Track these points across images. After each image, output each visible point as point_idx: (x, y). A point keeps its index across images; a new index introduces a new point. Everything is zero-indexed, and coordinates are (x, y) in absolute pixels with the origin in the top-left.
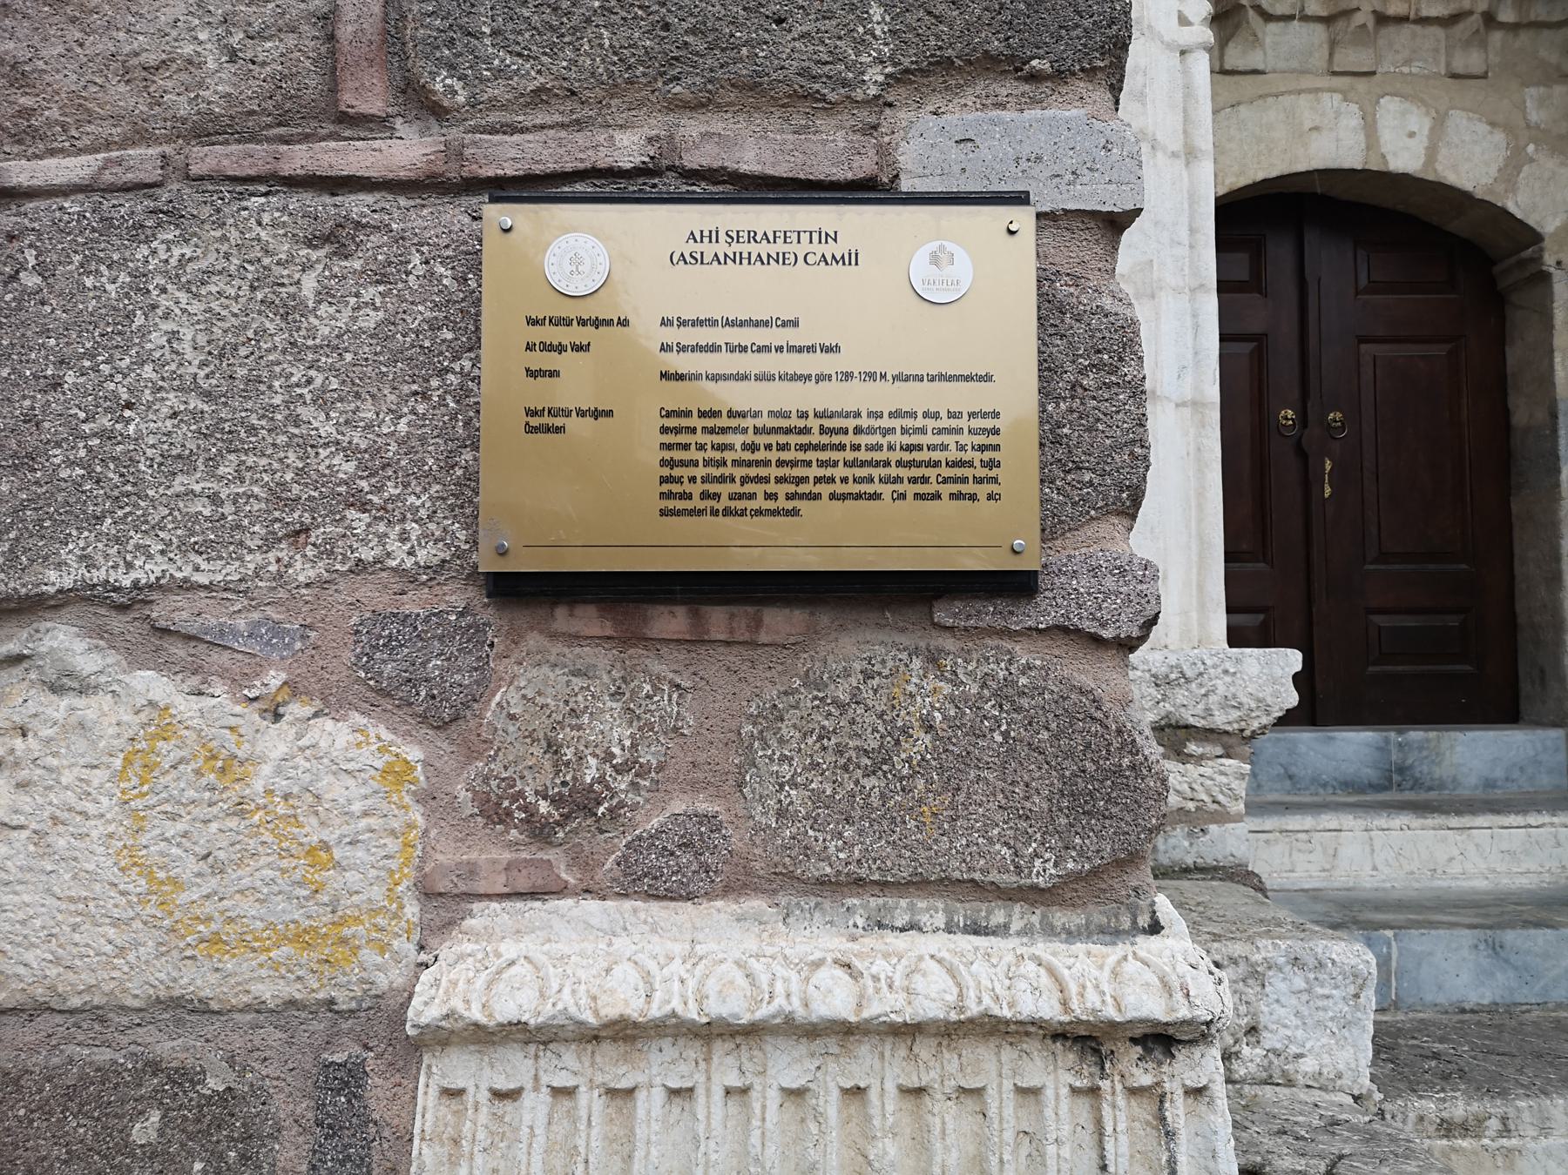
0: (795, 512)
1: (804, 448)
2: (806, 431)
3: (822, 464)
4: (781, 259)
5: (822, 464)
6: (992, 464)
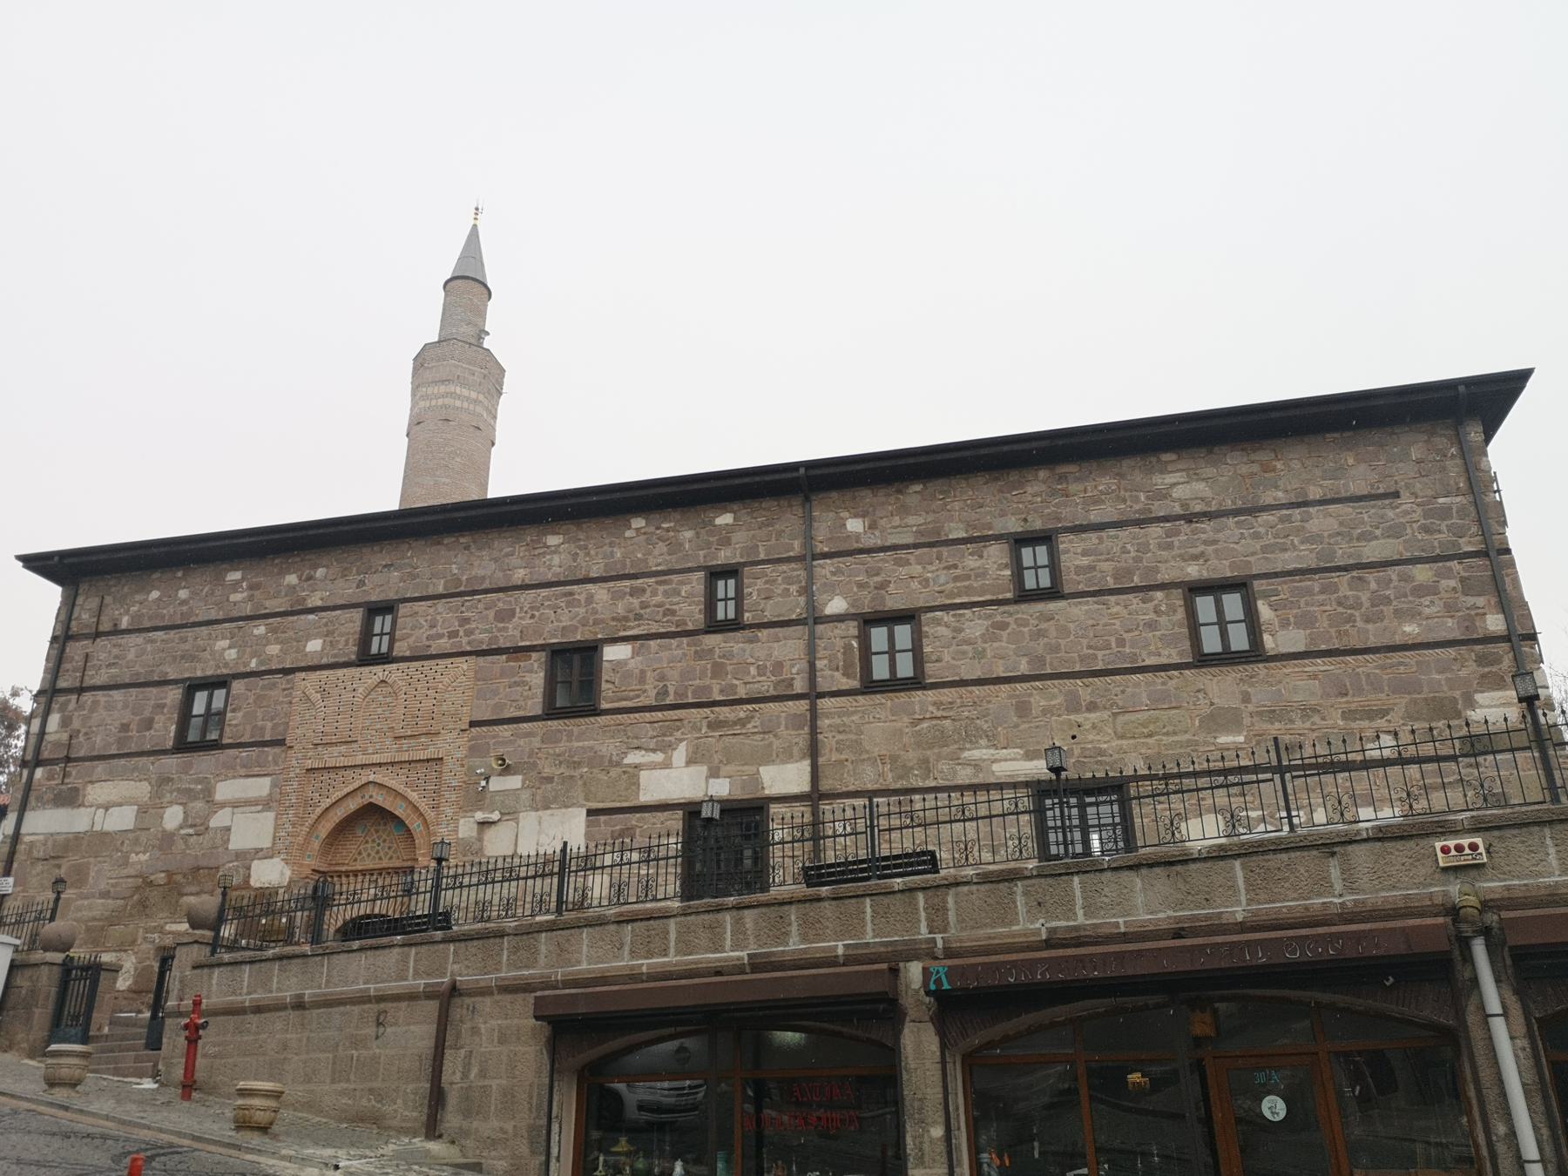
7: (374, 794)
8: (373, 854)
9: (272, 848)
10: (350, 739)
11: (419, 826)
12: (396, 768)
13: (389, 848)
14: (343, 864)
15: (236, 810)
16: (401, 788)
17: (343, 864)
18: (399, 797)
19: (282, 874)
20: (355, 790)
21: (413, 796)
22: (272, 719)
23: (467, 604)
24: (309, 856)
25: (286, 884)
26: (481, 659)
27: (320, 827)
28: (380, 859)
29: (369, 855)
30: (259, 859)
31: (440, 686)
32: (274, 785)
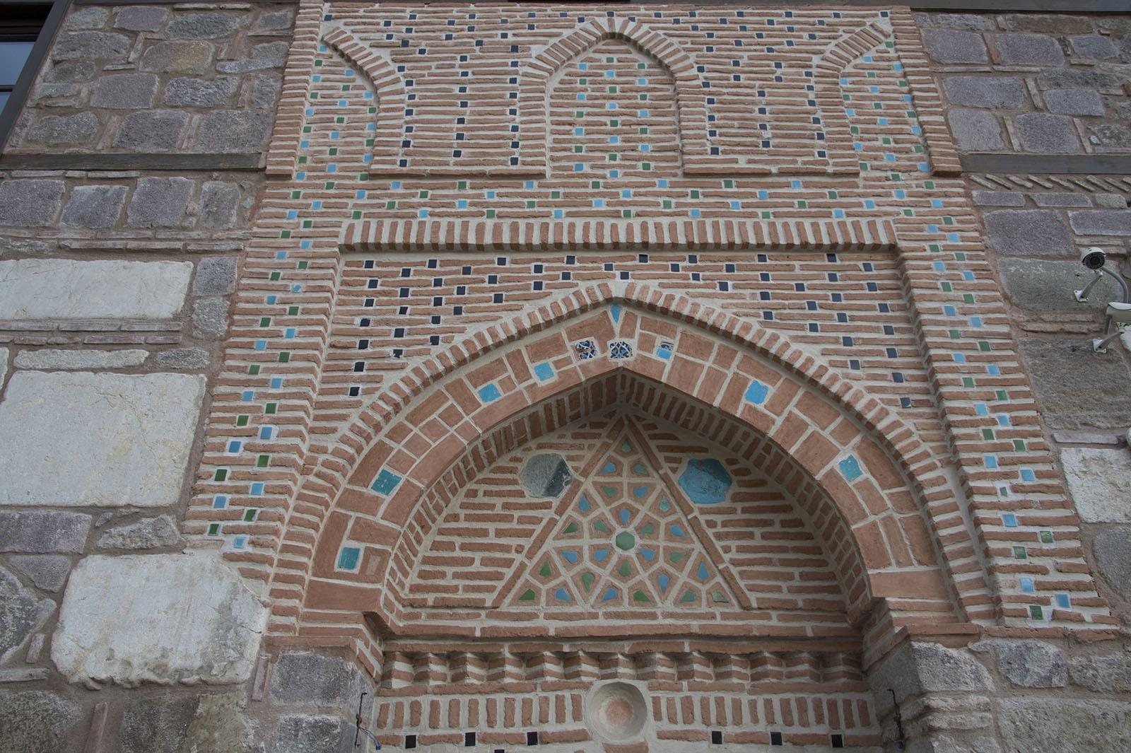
7: (633, 343)
8: (605, 575)
9: (179, 510)
11: (850, 464)
12: (711, 266)
13: (677, 558)
14: (479, 605)
15: (24, 358)
16: (752, 329)
19: (227, 622)
21: (810, 355)
25: (243, 672)
28: (640, 596)
29: (587, 580)
30: (114, 552)
31: (816, 60)
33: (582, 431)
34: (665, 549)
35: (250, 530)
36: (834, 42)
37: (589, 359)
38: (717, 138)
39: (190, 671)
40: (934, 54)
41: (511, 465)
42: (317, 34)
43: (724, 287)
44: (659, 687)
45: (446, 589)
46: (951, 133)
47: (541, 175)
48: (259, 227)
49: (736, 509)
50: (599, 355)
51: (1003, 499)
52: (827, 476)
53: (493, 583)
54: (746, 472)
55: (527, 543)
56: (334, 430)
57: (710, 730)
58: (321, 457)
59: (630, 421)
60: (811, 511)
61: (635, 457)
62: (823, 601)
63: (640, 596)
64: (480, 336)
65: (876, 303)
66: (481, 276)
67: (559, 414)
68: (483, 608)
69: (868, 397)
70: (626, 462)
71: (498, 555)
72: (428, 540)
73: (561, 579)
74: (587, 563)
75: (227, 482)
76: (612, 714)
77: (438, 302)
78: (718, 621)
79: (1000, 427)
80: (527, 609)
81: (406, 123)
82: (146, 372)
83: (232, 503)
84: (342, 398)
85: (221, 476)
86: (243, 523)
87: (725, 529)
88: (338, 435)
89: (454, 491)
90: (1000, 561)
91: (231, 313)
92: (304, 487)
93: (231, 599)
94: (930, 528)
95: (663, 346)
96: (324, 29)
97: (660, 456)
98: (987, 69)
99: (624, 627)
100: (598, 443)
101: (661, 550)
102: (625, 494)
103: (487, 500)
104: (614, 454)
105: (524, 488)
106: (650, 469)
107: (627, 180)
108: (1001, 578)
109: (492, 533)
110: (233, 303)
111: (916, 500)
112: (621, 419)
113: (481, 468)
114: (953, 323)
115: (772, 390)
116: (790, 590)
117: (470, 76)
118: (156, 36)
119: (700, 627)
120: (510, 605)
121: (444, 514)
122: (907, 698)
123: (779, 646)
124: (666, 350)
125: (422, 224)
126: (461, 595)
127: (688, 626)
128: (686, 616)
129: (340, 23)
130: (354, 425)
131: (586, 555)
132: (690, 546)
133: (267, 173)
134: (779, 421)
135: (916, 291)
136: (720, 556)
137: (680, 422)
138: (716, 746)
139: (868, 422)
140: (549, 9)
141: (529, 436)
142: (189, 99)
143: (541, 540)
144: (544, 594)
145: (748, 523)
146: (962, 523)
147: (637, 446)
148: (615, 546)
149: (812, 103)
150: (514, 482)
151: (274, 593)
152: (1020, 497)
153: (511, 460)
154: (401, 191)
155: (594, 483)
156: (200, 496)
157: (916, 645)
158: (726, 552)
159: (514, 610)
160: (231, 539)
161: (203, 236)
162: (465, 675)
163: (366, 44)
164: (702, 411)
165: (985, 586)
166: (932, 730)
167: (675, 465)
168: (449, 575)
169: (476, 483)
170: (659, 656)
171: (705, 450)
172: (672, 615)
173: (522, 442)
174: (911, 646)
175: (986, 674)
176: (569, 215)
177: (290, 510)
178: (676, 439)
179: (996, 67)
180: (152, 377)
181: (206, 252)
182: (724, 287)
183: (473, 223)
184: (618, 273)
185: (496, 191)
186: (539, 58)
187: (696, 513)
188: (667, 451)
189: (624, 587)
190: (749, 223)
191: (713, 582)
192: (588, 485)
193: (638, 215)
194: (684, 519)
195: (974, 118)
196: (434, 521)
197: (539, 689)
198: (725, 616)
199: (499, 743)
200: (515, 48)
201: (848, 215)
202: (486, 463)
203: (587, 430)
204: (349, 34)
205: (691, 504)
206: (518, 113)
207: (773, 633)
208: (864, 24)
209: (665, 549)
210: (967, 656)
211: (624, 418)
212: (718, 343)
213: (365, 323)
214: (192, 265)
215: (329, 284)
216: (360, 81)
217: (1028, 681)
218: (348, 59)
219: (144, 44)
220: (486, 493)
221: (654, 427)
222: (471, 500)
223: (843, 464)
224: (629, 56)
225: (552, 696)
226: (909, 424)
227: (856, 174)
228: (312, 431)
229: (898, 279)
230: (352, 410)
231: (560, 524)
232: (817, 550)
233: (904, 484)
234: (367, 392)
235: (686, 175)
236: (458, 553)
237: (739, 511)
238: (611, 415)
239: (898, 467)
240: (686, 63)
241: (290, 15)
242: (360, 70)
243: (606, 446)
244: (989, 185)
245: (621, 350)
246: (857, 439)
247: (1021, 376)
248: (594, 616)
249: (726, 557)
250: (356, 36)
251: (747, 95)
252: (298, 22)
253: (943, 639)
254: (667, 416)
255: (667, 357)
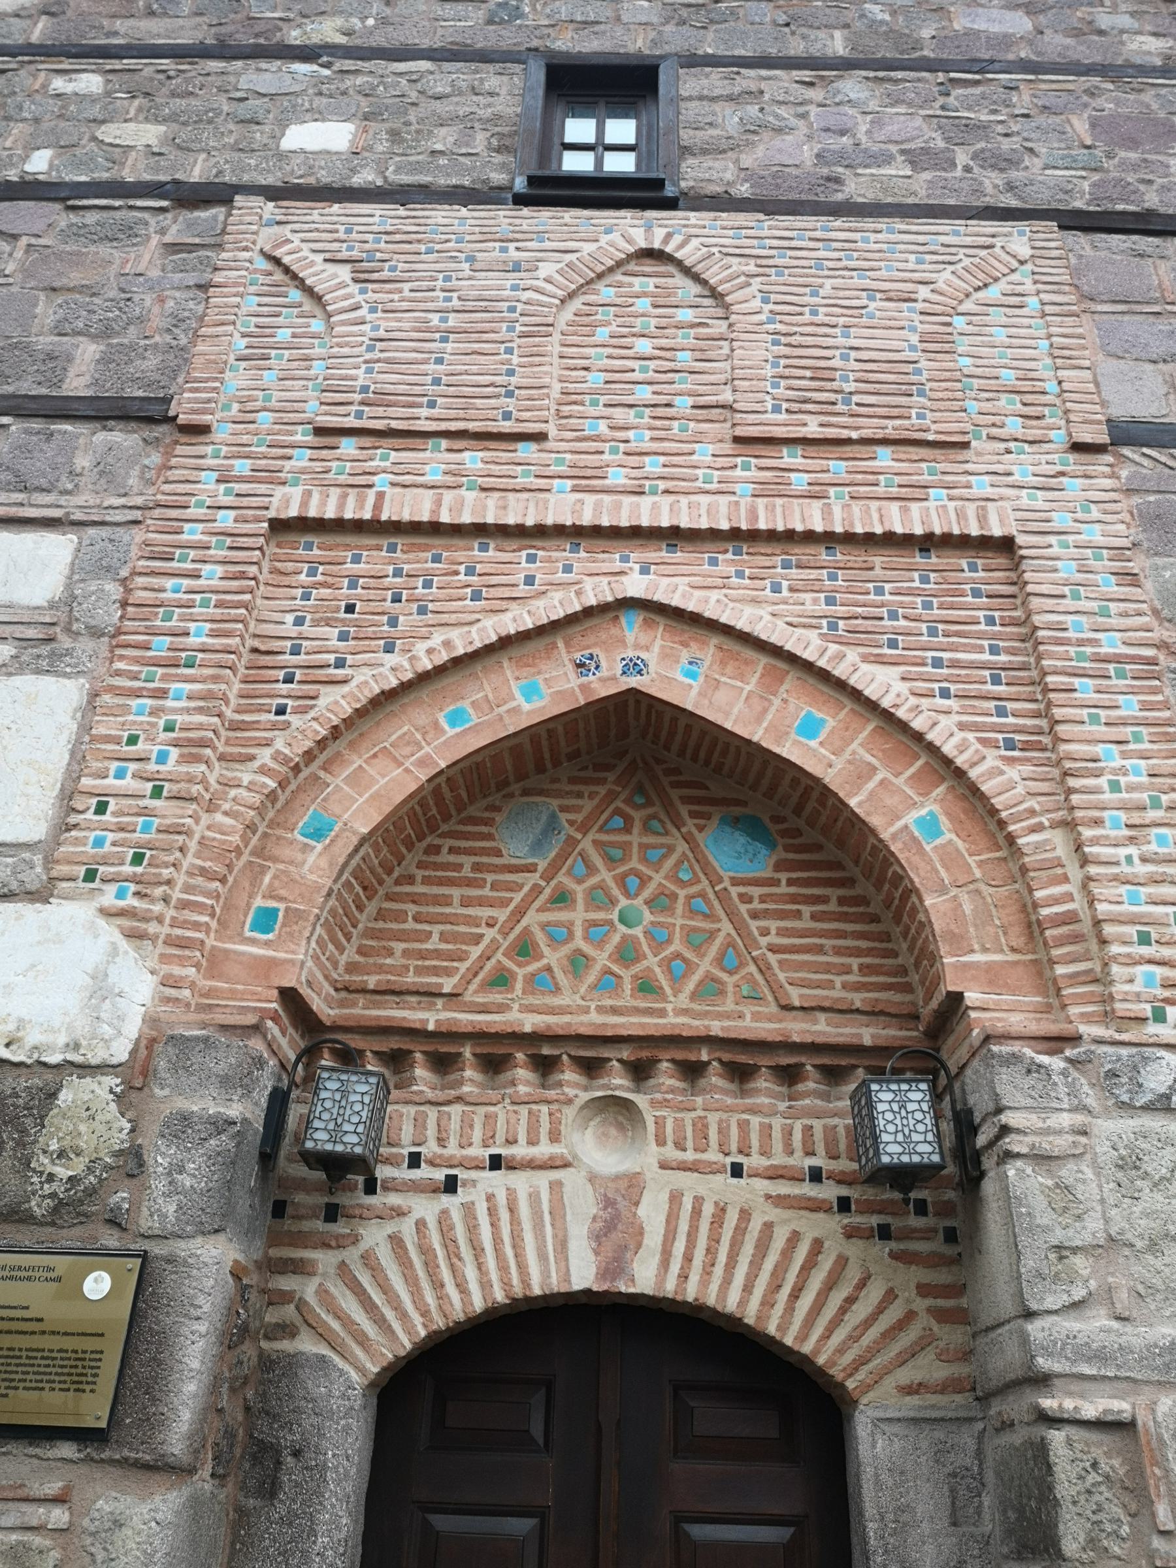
0: (6, 1396)
1: (17, 1365)
2: (20, 1357)
3: (24, 1373)
4: (29, 1279)
5: (24, 1373)
6: (96, 1375)
7: (651, 657)
8: (602, 958)
9: (49, 849)
10: (507, 426)
11: (931, 826)
13: (698, 941)
14: (432, 994)
17: (432, 994)
18: (792, 680)
20: (541, 631)
22: (106, 332)
23: (959, 92)
24: (266, 920)
25: (120, 1052)
26: (1081, 241)
27: (337, 780)
28: (646, 986)
29: (578, 963)
32: (80, 571)
33: (582, 774)
34: (682, 927)
35: (135, 879)
36: (950, 268)
37: (591, 677)
38: (781, 390)
39: (50, 1048)
40: (1086, 288)
41: (486, 815)
42: (254, 243)
43: (776, 589)
44: (665, 1104)
45: (390, 970)
46: (1099, 392)
47: (540, 437)
48: (164, 494)
49: (779, 881)
50: (604, 672)
51: (1126, 869)
52: (894, 836)
53: (455, 964)
54: (798, 833)
55: (502, 915)
56: (252, 758)
57: (728, 1160)
58: (233, 793)
59: (646, 763)
60: (878, 885)
61: (650, 811)
62: (889, 1001)
63: (646, 986)
64: (447, 644)
65: (981, 614)
66: (455, 567)
67: (551, 750)
68: (441, 995)
69: (959, 736)
70: (637, 816)
71: (462, 929)
72: (371, 908)
73: (545, 961)
74: (579, 942)
75: (107, 817)
76: (602, 1138)
77: (397, 599)
78: (748, 1022)
79: (1132, 779)
80: (497, 997)
81: (366, 362)
82: (10, 674)
83: (114, 844)
84: (264, 717)
85: (101, 809)
86: (128, 869)
87: (764, 906)
88: (256, 764)
89: (410, 847)
90: (1115, 949)
91: (124, 604)
92: (209, 828)
93: (108, 962)
94: (1030, 905)
95: (690, 663)
96: (266, 238)
97: (684, 810)
98: (1156, 309)
99: (622, 1025)
100: (602, 790)
101: (678, 929)
102: (635, 856)
103: (452, 858)
104: (622, 805)
105: (501, 846)
106: (669, 826)
107: (655, 446)
108: (1115, 969)
109: (456, 901)
110: (128, 591)
111: (1015, 869)
112: (634, 761)
113: (446, 818)
114: (1081, 643)
115: (831, 723)
116: (845, 986)
117: (456, 303)
118: (42, 241)
119: (722, 1028)
120: (476, 992)
121: (396, 874)
122: (984, 1120)
123: (826, 1060)
124: (694, 668)
125: (381, 496)
126: (411, 979)
127: (707, 1028)
128: (705, 1015)
129: (286, 230)
130: (278, 752)
131: (578, 932)
132: (716, 926)
133: (179, 421)
134: (839, 763)
135: (1035, 602)
136: (755, 940)
137: (712, 766)
138: (735, 1181)
139: (957, 768)
140: (566, 215)
141: (512, 778)
142: (81, 325)
143: (520, 912)
144: (520, 978)
145: (794, 899)
146: (1073, 900)
147: (654, 797)
148: (616, 922)
149: (913, 348)
150: (489, 837)
151: (164, 959)
152: (1150, 868)
153: (486, 809)
154: (354, 452)
155: (594, 842)
156: (73, 833)
157: (995, 1048)
158: (762, 935)
159: (480, 999)
160: (112, 889)
161: (91, 503)
162: (413, 1080)
163: (319, 258)
164: (738, 749)
165: (1096, 981)
166: (1009, 1155)
167: (702, 822)
168: (398, 953)
169: (439, 836)
170: (665, 1065)
171: (743, 803)
172: (685, 1012)
173: (503, 784)
174: (989, 1050)
175: (1086, 1088)
176: (575, 490)
177: (190, 855)
178: (707, 788)
179: (1169, 307)
180: (17, 680)
181: (95, 523)
182: (776, 589)
183: (448, 496)
184: (637, 567)
185: (481, 454)
186: (548, 280)
187: (726, 883)
188: (692, 804)
189: (626, 975)
190: (817, 504)
191: (743, 972)
192: (586, 844)
193: (667, 492)
194: (709, 890)
195: (1133, 374)
196: (381, 882)
197: (507, 1101)
198: (756, 1017)
199: (451, 1167)
200: (517, 268)
201: (951, 499)
202: (453, 812)
203: (589, 773)
204: (297, 243)
205: (721, 872)
206: (516, 352)
207: (820, 1040)
208: (991, 247)
209: (682, 927)
210: (1062, 1065)
211: (639, 760)
212: (763, 660)
213: (299, 622)
214: (76, 540)
215: (253, 570)
216: (308, 307)
217: (1141, 1101)
218: (295, 277)
219: (27, 252)
220: (451, 850)
221: (677, 771)
222: (433, 858)
223: (920, 821)
224: (669, 280)
225: (524, 1110)
226: (1013, 773)
227: (965, 445)
228: (222, 758)
229: (1014, 584)
230: (276, 733)
231: (548, 891)
232: (886, 937)
233: (1000, 849)
234: (298, 711)
235: (737, 440)
236: (410, 925)
237: (784, 882)
238: (622, 755)
239: (993, 827)
240: (747, 290)
241: (221, 218)
242: (309, 291)
243: (611, 796)
244: (1146, 462)
245: (634, 667)
246: (941, 789)
247: (1166, 714)
248: (587, 1011)
249: (764, 941)
250: (304, 246)
251: (826, 336)
252: (229, 228)
253: (1033, 1043)
254: (695, 759)
255: (693, 676)
